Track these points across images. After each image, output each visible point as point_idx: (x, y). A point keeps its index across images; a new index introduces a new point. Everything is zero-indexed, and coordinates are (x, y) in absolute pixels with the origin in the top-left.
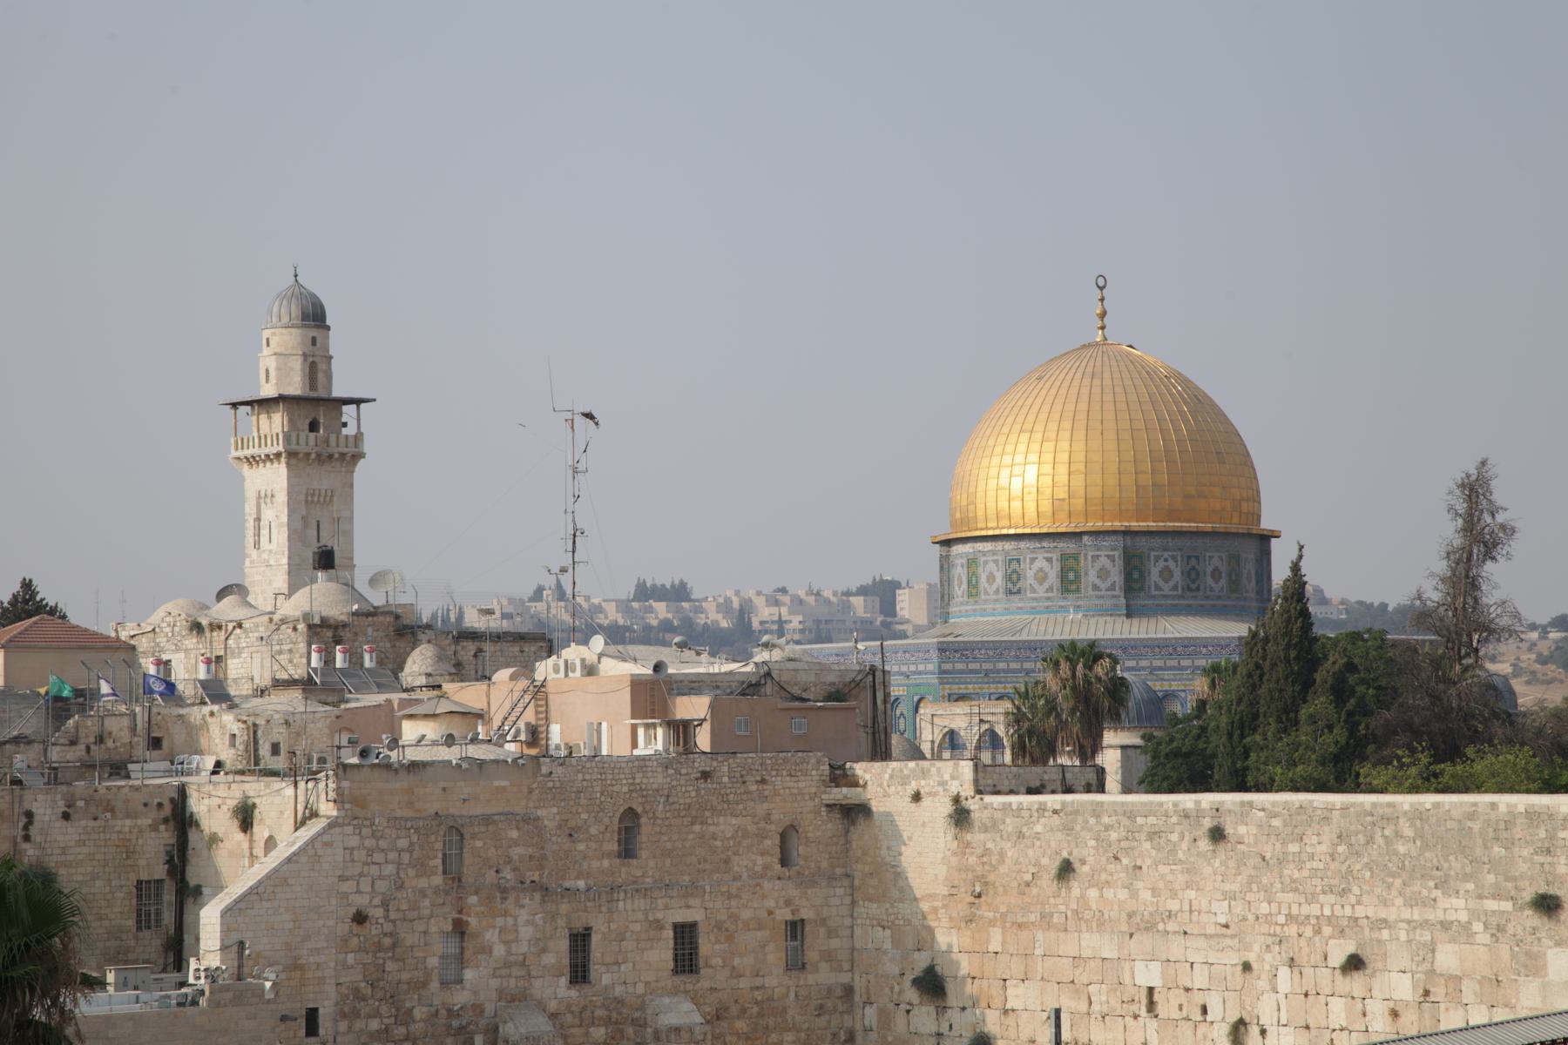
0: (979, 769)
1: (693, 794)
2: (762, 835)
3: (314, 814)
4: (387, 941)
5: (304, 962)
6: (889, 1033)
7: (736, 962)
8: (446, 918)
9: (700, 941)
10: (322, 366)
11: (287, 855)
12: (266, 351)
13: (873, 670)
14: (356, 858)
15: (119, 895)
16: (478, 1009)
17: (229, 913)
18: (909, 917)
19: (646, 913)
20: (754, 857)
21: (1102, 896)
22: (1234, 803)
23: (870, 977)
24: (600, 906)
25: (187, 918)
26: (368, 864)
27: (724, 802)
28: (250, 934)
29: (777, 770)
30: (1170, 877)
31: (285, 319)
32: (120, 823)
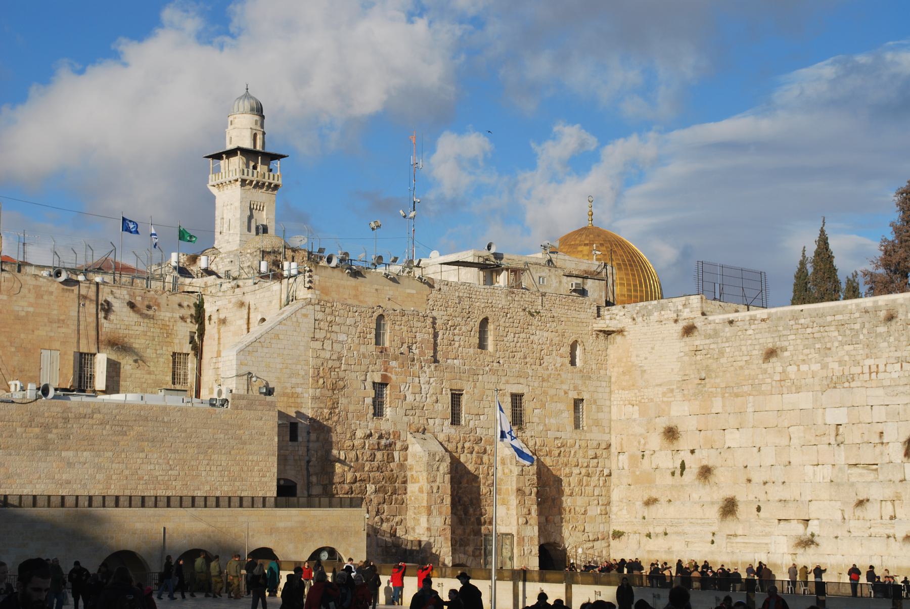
0: (704, 301)
2: (560, 345)
3: (294, 298)
4: (341, 383)
6: (637, 469)
10: (259, 137)
12: (230, 127)
15: (161, 360)
16: (397, 435)
18: (652, 397)
21: (799, 370)
22: (905, 299)
23: (623, 436)
24: (469, 377)
30: (854, 353)
31: (241, 110)
32: (162, 314)
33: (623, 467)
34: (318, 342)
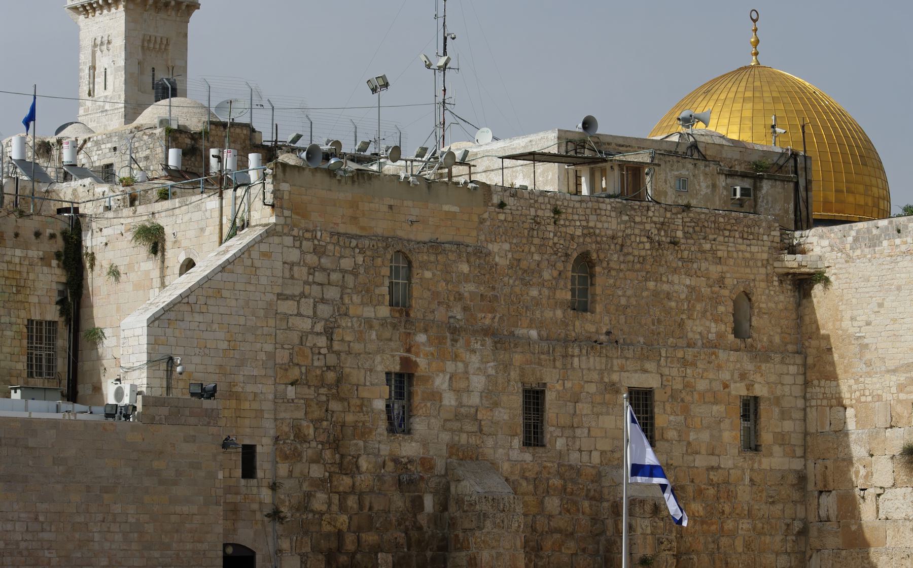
1: (648, 246)
2: (716, 300)
4: (331, 376)
5: (240, 390)
7: (692, 436)
8: (393, 356)
9: (656, 410)
11: (220, 262)
13: (795, 155)
14: (296, 276)
16: (426, 463)
17: (157, 322)
18: (880, 392)
19: (601, 373)
20: (708, 323)
24: (554, 360)
25: (85, 366)
26: (309, 284)
27: (679, 259)
28: (180, 350)
29: (730, 231)
32: (9, 252)
33: (828, 517)
34: (290, 302)
